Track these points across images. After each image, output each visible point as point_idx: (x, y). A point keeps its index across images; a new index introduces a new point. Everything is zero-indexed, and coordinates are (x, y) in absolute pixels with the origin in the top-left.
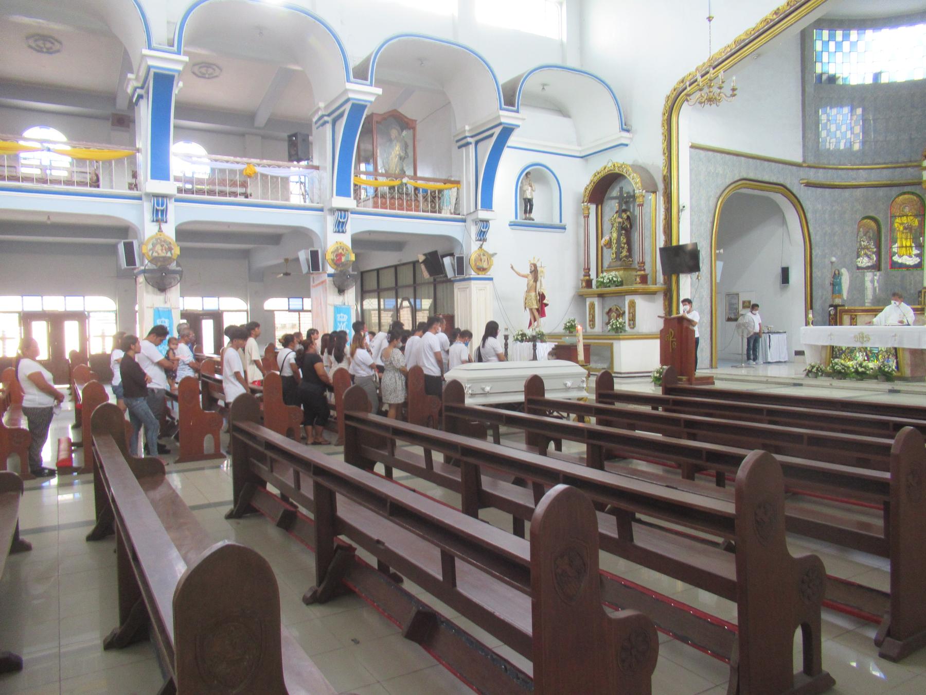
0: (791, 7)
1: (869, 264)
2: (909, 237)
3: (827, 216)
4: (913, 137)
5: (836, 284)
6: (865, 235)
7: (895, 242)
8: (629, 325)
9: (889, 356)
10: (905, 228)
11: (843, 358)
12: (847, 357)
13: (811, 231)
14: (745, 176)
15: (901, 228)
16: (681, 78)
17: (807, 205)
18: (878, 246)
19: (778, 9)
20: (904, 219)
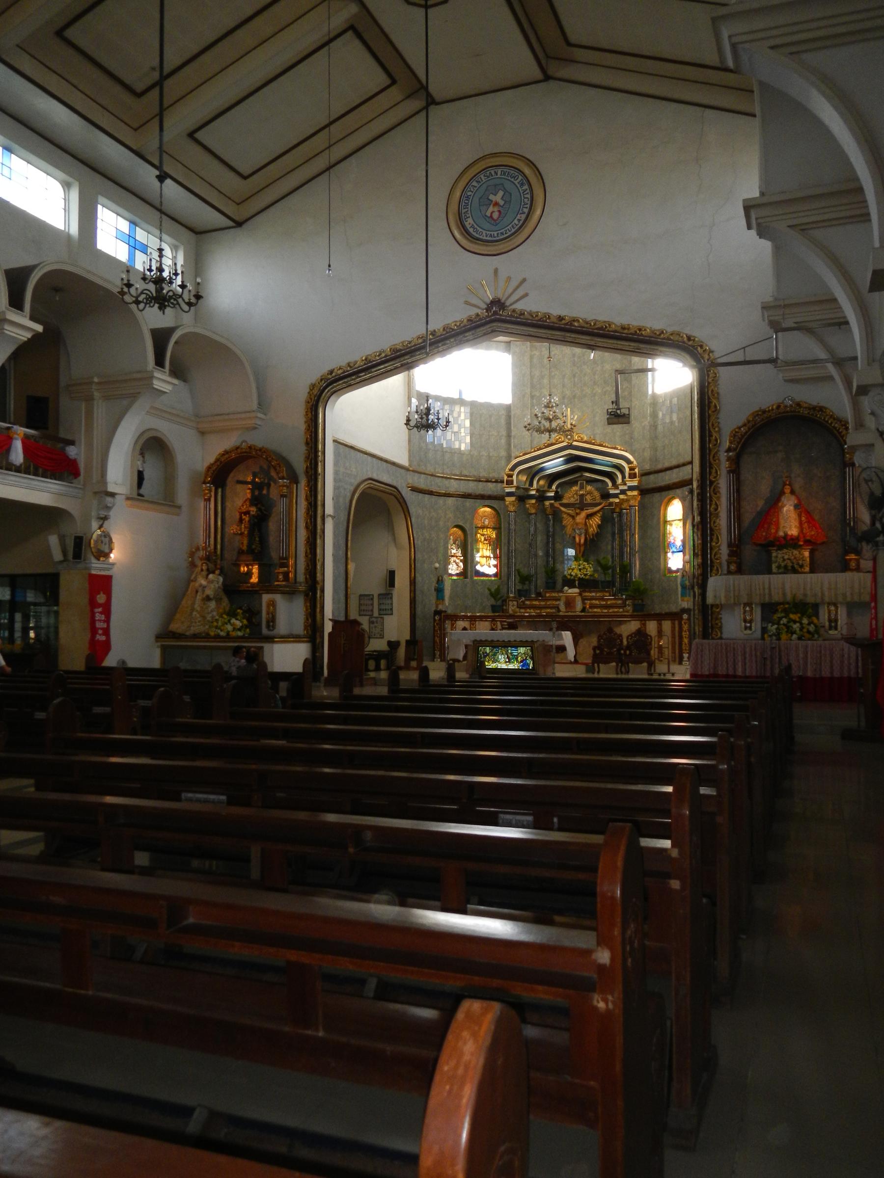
0: (447, 333)
1: (458, 572)
2: (488, 548)
3: (426, 522)
4: (491, 455)
5: (439, 591)
6: (454, 543)
7: (478, 551)
8: (268, 627)
9: (526, 657)
10: (485, 540)
13: (415, 535)
14: (370, 476)
15: (483, 539)
16: (330, 368)
17: (413, 510)
18: (465, 554)
19: (435, 331)
20: (485, 531)
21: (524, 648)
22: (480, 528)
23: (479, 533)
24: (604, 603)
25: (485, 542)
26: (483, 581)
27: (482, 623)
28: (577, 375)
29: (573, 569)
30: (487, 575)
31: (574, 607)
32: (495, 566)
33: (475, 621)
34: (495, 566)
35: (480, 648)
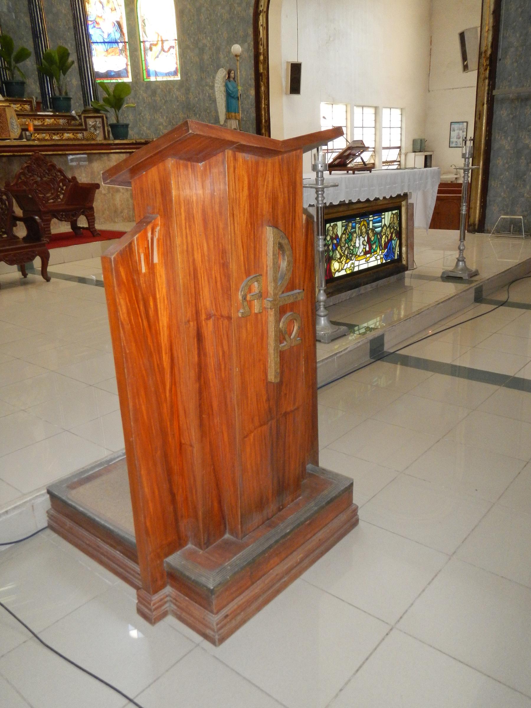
11: (338, 256)
12: (344, 253)
21: (390, 213)
35: (328, 225)
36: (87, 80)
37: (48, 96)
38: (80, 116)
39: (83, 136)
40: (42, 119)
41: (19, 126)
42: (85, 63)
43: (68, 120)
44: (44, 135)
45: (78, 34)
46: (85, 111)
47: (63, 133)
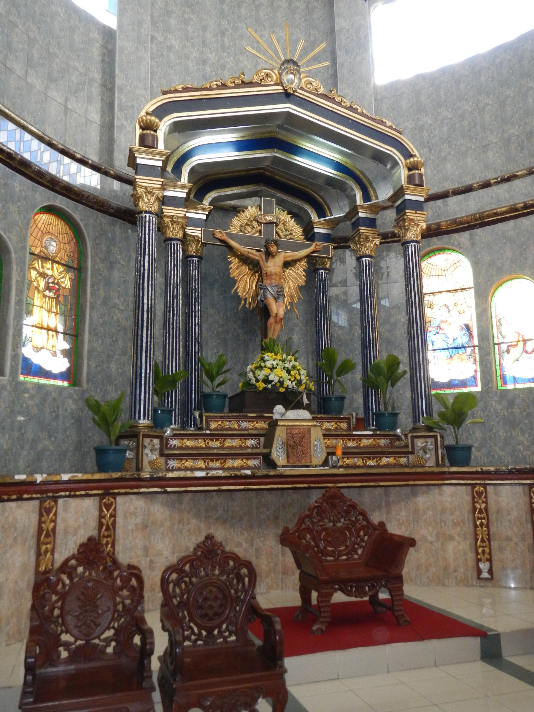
10: (48, 288)
15: (42, 285)
22: (38, 257)
23: (35, 269)
24: (355, 444)
25: (47, 293)
26: (40, 387)
27: (73, 503)
28: (227, 33)
29: (272, 369)
30: (48, 375)
31: (306, 453)
32: (65, 352)
33: (55, 499)
34: (65, 352)
36: (419, 391)
37: (371, 412)
38: (406, 435)
39: (408, 460)
40: (358, 439)
41: (325, 449)
42: (418, 372)
43: (391, 440)
44: (356, 460)
45: (413, 341)
46: (414, 429)
47: (381, 457)
